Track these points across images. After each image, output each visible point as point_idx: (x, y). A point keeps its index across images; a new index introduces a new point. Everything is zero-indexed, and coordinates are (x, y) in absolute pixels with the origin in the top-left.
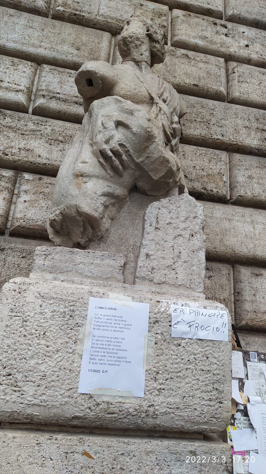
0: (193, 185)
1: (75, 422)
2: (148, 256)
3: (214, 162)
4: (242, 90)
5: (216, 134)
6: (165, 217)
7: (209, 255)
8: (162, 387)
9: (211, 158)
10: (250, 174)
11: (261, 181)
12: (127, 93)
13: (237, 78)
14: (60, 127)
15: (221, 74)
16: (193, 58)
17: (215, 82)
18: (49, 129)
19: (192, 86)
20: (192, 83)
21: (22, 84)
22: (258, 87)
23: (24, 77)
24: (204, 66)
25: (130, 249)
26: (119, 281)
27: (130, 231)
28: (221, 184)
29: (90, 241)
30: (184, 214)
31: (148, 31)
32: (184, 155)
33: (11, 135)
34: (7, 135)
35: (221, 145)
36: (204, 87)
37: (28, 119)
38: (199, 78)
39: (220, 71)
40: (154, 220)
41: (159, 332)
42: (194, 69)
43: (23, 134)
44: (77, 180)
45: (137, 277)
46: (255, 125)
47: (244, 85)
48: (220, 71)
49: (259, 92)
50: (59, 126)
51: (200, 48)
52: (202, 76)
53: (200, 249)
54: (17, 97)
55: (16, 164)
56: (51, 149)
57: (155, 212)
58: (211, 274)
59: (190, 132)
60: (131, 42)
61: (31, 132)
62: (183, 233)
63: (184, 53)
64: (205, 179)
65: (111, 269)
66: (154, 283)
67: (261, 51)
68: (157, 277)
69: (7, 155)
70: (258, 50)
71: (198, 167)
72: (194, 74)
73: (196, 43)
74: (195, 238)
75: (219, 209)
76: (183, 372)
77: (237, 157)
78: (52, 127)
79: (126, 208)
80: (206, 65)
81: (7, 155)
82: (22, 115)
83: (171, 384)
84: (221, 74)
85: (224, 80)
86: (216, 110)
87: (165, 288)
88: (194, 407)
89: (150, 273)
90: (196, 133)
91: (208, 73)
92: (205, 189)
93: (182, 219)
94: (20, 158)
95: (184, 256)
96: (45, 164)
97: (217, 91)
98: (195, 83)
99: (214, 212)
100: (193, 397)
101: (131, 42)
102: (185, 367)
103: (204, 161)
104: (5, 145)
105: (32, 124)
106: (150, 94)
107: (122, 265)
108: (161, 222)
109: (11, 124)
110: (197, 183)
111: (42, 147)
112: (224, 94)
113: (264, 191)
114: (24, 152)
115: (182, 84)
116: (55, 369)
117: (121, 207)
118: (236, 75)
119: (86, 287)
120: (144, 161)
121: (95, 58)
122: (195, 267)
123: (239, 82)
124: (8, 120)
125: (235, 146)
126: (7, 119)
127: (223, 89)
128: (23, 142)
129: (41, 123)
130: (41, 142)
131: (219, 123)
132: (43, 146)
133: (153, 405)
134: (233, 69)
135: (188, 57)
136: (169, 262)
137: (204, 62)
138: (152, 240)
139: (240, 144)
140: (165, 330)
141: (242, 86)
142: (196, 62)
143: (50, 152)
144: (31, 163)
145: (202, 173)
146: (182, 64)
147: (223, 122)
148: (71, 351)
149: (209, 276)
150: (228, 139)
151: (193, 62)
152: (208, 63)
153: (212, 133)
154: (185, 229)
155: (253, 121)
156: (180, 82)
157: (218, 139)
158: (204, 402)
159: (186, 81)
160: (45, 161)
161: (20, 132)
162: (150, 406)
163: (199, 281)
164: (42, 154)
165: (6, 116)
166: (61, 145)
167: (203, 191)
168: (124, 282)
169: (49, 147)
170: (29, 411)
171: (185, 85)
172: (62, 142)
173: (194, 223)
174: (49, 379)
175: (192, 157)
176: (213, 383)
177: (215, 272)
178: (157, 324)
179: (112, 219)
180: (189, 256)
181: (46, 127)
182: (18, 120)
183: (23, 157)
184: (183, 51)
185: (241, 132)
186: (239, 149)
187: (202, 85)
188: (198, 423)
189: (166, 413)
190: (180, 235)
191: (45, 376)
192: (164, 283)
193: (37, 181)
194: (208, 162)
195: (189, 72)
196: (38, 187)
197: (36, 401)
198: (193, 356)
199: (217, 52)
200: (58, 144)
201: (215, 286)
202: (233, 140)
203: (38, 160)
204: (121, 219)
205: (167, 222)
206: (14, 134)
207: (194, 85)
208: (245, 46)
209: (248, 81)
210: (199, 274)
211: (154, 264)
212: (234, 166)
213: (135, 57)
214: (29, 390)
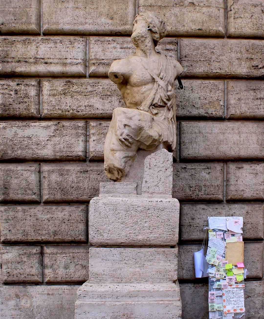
0: (199, 112)
1: (122, 244)
2: (146, 182)
3: (214, 91)
5: (215, 69)
6: (153, 162)
8: (152, 231)
9: (212, 88)
14: (107, 85)
15: (220, 15)
16: (197, 5)
17: (215, 24)
18: (101, 88)
20: (197, 28)
21: (79, 58)
23: (79, 52)
26: (135, 194)
28: (218, 108)
29: (122, 177)
30: (162, 160)
32: (192, 90)
33: (79, 97)
34: (77, 98)
35: (220, 76)
37: (87, 83)
38: (202, 22)
39: (219, 12)
40: (148, 165)
41: (150, 213)
42: (198, 15)
43: (85, 95)
45: (142, 192)
48: (219, 12)
49: (250, 25)
50: (106, 85)
52: (205, 20)
53: (170, 175)
54: (77, 69)
55: (85, 116)
56: (104, 102)
57: (149, 160)
58: (210, 171)
59: (196, 70)
61: (90, 92)
62: (162, 169)
64: (207, 106)
65: (131, 189)
66: (150, 193)
68: (151, 190)
69: (79, 112)
71: (202, 98)
72: (199, 20)
74: (168, 170)
75: (216, 127)
76: (160, 226)
77: (232, 83)
78: (102, 86)
79: (136, 160)
81: (79, 112)
82: (83, 80)
83: (155, 230)
84: (220, 15)
85: (222, 20)
86: (216, 48)
87: (154, 195)
88: (164, 237)
89: (147, 189)
90: (200, 71)
91: (210, 16)
92: (207, 113)
93: (162, 162)
94: (86, 113)
95: (163, 180)
96: (102, 113)
97: (216, 31)
98: (200, 27)
99: (213, 129)
100: (163, 234)
102: (160, 224)
103: (206, 92)
104: (76, 105)
105: (90, 87)
107: (136, 187)
108: (151, 165)
109: (77, 90)
110: (201, 110)
111: (98, 102)
112: (222, 33)
113: (249, 108)
114: (88, 108)
116: (113, 228)
117: (133, 160)
118: (232, 12)
119: (121, 198)
122: (167, 184)
124: (75, 87)
126: (74, 87)
127: (221, 29)
128: (87, 101)
129: (95, 85)
130: (97, 99)
131: (218, 59)
132: (99, 101)
133: (149, 237)
135: (194, 5)
136: (156, 183)
138: (148, 174)
140: (152, 212)
141: (237, 21)
142: (200, 8)
143: (103, 105)
144: (93, 114)
145: (205, 101)
147: (221, 57)
148: (118, 222)
151: (198, 8)
152: (210, 6)
153: (212, 69)
154: (163, 167)
157: (216, 73)
158: (168, 235)
160: (101, 112)
161: (83, 94)
162: (147, 238)
163: (169, 190)
164: (99, 107)
165: (74, 84)
166: (110, 98)
167: (206, 115)
168: (137, 194)
169: (102, 101)
170: (107, 241)
171: (192, 31)
172: (110, 96)
173: (167, 163)
174: (111, 232)
175: (198, 90)
176: (171, 229)
177: (212, 170)
178: (149, 210)
179: (130, 166)
180: (165, 179)
181: (99, 87)
182: (81, 86)
183: (87, 112)
187: (205, 28)
188: (166, 242)
189: (153, 240)
190: (161, 170)
191: (110, 230)
192: (154, 192)
193: (99, 126)
194: (209, 92)
195: (195, 18)
196: (99, 130)
197: (108, 238)
198: (163, 220)
200: (108, 98)
203: (97, 112)
204: (134, 166)
205: (154, 165)
206: (80, 97)
210: (169, 187)
211: (149, 185)
214: (105, 235)
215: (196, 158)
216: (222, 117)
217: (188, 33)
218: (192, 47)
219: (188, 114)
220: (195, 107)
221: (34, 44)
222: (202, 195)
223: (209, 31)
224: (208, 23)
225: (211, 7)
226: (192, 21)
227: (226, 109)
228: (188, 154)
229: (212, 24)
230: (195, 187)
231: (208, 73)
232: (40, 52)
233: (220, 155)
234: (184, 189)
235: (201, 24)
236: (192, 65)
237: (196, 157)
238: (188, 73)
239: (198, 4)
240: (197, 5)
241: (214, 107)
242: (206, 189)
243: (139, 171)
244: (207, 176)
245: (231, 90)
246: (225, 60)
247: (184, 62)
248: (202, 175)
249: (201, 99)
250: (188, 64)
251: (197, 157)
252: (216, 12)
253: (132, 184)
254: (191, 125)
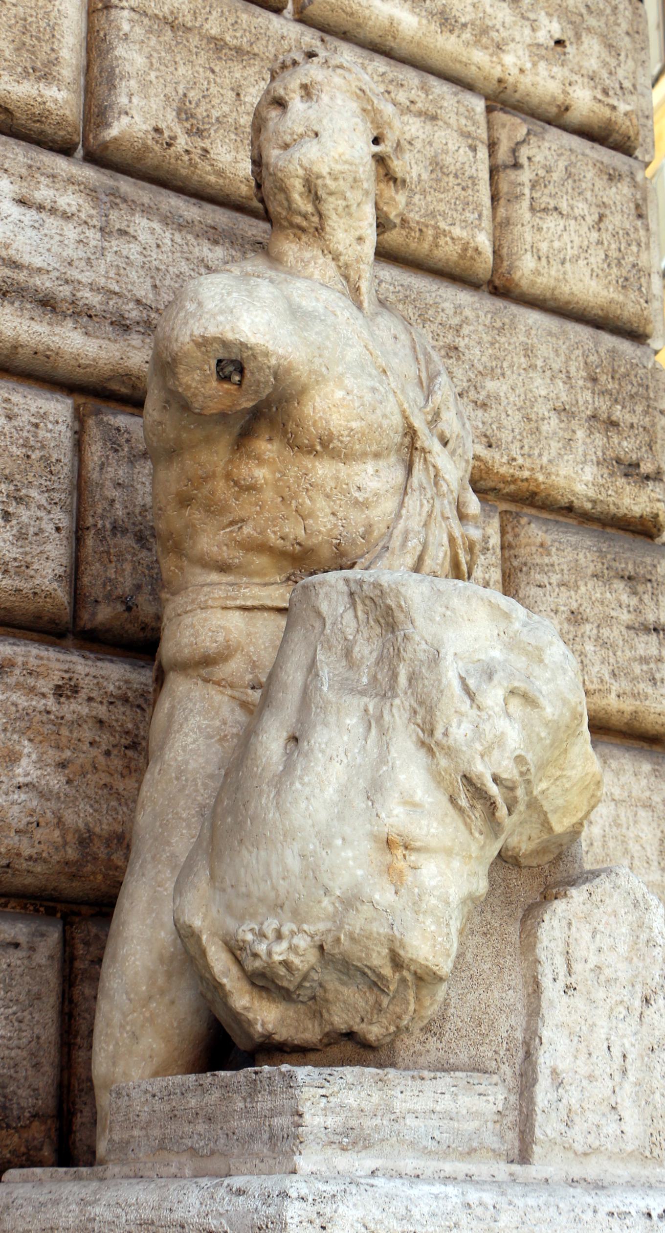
4: (544, 247)
10: (574, 606)
11: (605, 632)
12: (354, 425)
13: (527, 191)
17: (459, 208)
22: (594, 235)
24: (421, 131)
25: (502, 1053)
27: (496, 993)
31: (376, 141)
36: (424, 229)
44: (388, 857)
46: (586, 399)
47: (551, 223)
48: (475, 157)
51: (404, 39)
60: (331, 194)
65: (476, 1124)
67: (605, 74)
70: (592, 64)
80: (428, 127)
86: (466, 330)
101: (331, 194)
106: (406, 418)
108: (577, 967)
118: (525, 176)
120: (548, 789)
121: (39, 64)
123: (532, 209)
125: (525, 484)
134: (514, 151)
137: (420, 114)
139: (541, 478)
150: (505, 459)
155: (581, 383)
185: (545, 428)
186: (534, 494)
199: (460, 62)
202: (520, 461)
208: (552, 43)
209: (564, 207)
212: (524, 569)
213: (341, 248)
223: (436, 237)
224: (429, 198)
225: (440, 123)
229: (442, 207)
243: (496, 995)
245: (538, 560)
246: (504, 402)
252: (461, 151)
253: (481, 1089)
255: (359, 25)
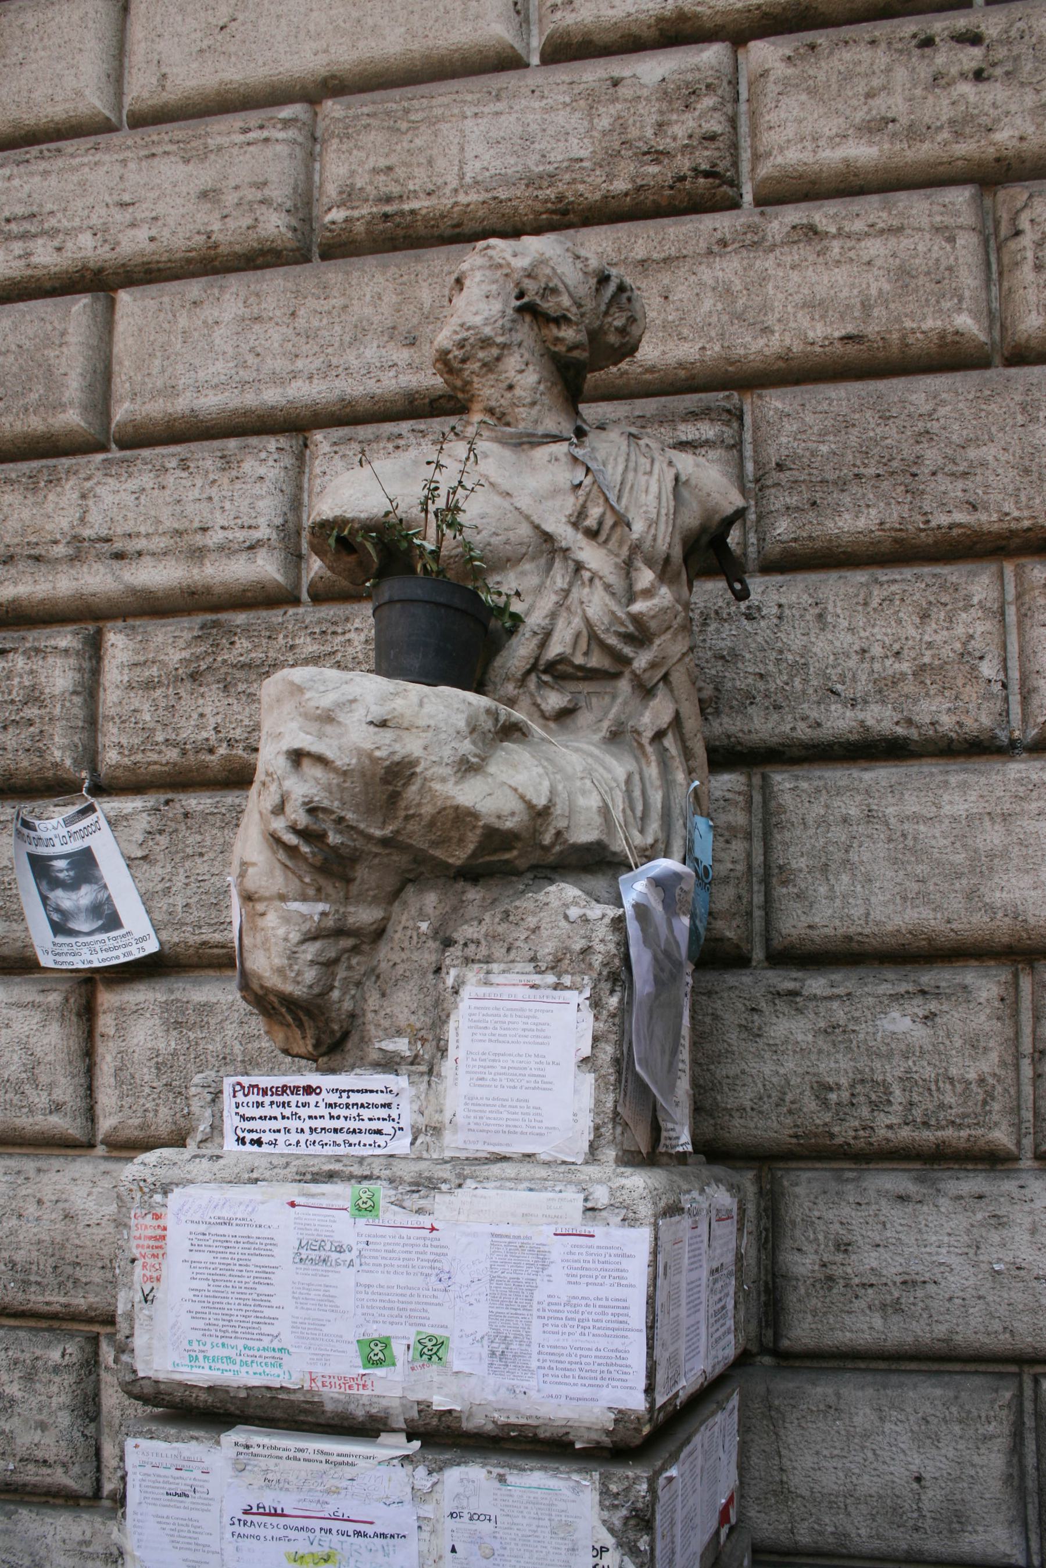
7: (930, 944)
16: (833, 230)
19: (838, 345)
20: (837, 334)
42: (840, 275)
63: (797, 221)
73: (846, 161)
115: (797, 347)
135: (816, 233)
142: (849, 244)
146: (793, 267)
149: (926, 1013)
151: (836, 246)
156: (788, 342)
159: (811, 334)
184: (793, 215)
195: (821, 292)
201: (947, 1042)
207: (847, 338)
215: (854, 945)
216: (995, 737)
217: (793, 363)
218: (809, 419)
219: (803, 732)
220: (839, 695)
221: (71, 483)
222: (890, 1127)
226: (805, 305)
227: (1015, 699)
228: (810, 927)
230: (852, 1086)
231: (904, 534)
232: (95, 517)
233: (992, 925)
234: (789, 1097)
235: (857, 314)
236: (814, 503)
237: (849, 938)
238: (795, 540)
239: (839, 229)
240: (833, 230)
241: (947, 693)
242: (916, 1098)
244: (920, 1034)
247: (773, 491)
248: (891, 1027)
249: (873, 658)
250: (793, 500)
251: (860, 938)
254: (821, 783)
255: (813, 183)
